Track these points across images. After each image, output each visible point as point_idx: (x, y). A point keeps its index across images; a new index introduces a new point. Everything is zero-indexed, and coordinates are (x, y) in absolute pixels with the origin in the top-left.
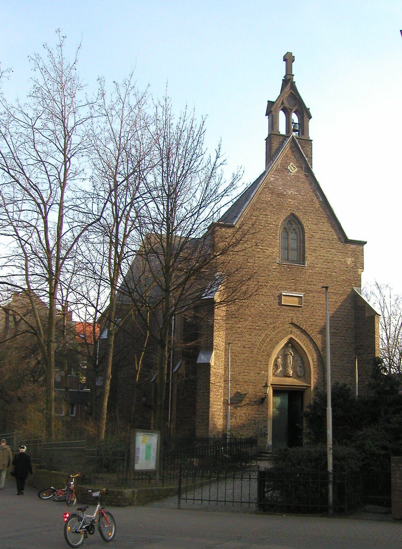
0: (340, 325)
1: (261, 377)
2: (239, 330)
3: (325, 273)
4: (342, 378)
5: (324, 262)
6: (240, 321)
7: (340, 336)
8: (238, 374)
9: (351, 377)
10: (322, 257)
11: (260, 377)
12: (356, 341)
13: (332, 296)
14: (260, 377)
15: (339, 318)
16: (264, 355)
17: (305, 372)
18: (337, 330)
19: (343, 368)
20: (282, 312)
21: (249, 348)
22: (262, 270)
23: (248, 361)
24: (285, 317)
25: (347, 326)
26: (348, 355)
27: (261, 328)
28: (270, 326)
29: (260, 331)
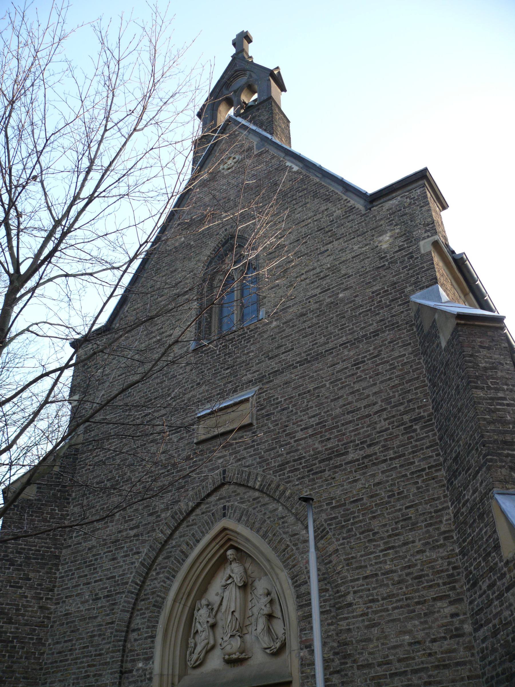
0: (378, 426)
4: (412, 618)
18: (369, 446)
26: (422, 518)
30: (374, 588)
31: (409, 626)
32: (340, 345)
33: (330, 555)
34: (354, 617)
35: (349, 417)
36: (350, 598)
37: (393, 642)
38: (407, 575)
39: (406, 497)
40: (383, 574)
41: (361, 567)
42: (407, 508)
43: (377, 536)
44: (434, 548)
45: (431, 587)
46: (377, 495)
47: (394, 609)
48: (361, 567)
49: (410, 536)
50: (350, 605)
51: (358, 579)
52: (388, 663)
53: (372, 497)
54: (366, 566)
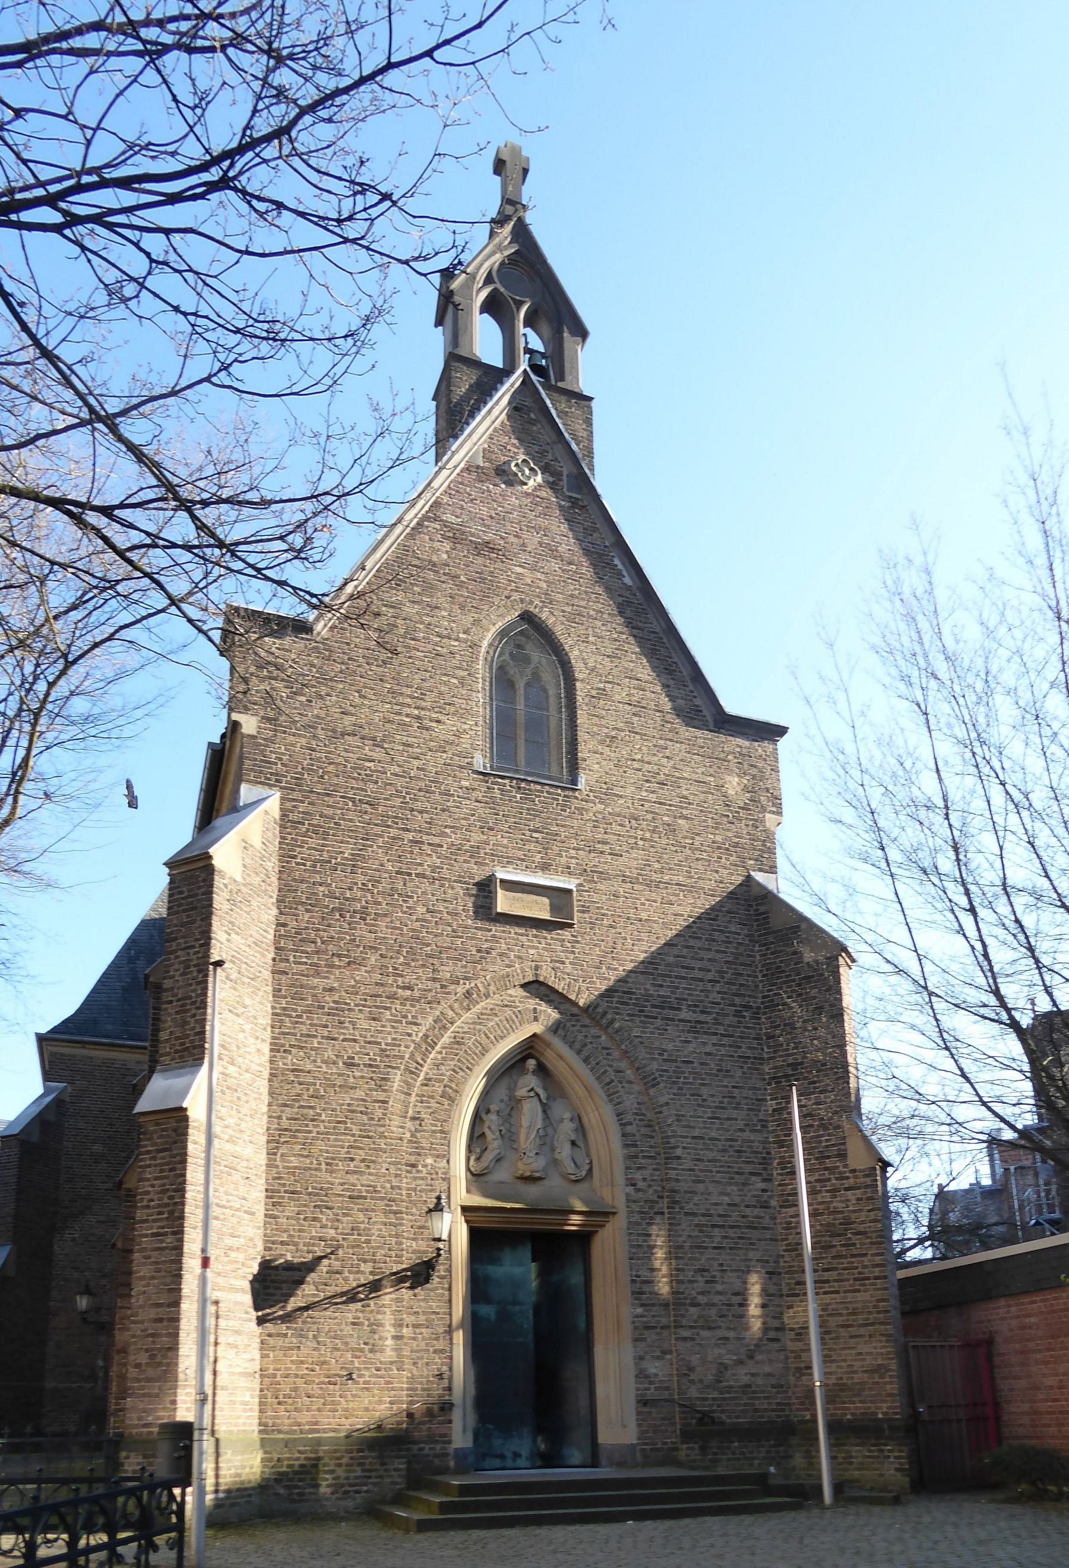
0: (711, 996)
1: (422, 1179)
2: (327, 998)
3: (649, 816)
5: (647, 781)
6: (333, 966)
7: (716, 1034)
8: (323, 1166)
9: (764, 1180)
10: (636, 765)
11: (415, 1178)
12: (775, 1052)
13: (678, 895)
14: (415, 1178)
15: (709, 971)
16: (432, 1097)
17: (591, 1163)
18: (702, 1012)
19: (731, 1146)
20: (497, 942)
21: (370, 1066)
22: (420, 790)
23: (365, 1117)
24: (511, 961)
25: (737, 1000)
27: (416, 993)
28: (452, 987)
29: (413, 1006)
30: (701, 1150)
31: (729, 1189)
32: (677, 884)
33: (661, 1106)
34: (683, 1170)
35: (683, 972)
36: (679, 1152)
37: (714, 1199)
38: (731, 1146)
39: (733, 1076)
40: (710, 1139)
41: (690, 1127)
42: (734, 1087)
43: (705, 1104)
44: (752, 1131)
45: (748, 1162)
46: (707, 1064)
47: (718, 1172)
48: (690, 1127)
49: (734, 1114)
50: (679, 1158)
51: (687, 1137)
52: (710, 1215)
53: (702, 1064)
54: (694, 1127)
